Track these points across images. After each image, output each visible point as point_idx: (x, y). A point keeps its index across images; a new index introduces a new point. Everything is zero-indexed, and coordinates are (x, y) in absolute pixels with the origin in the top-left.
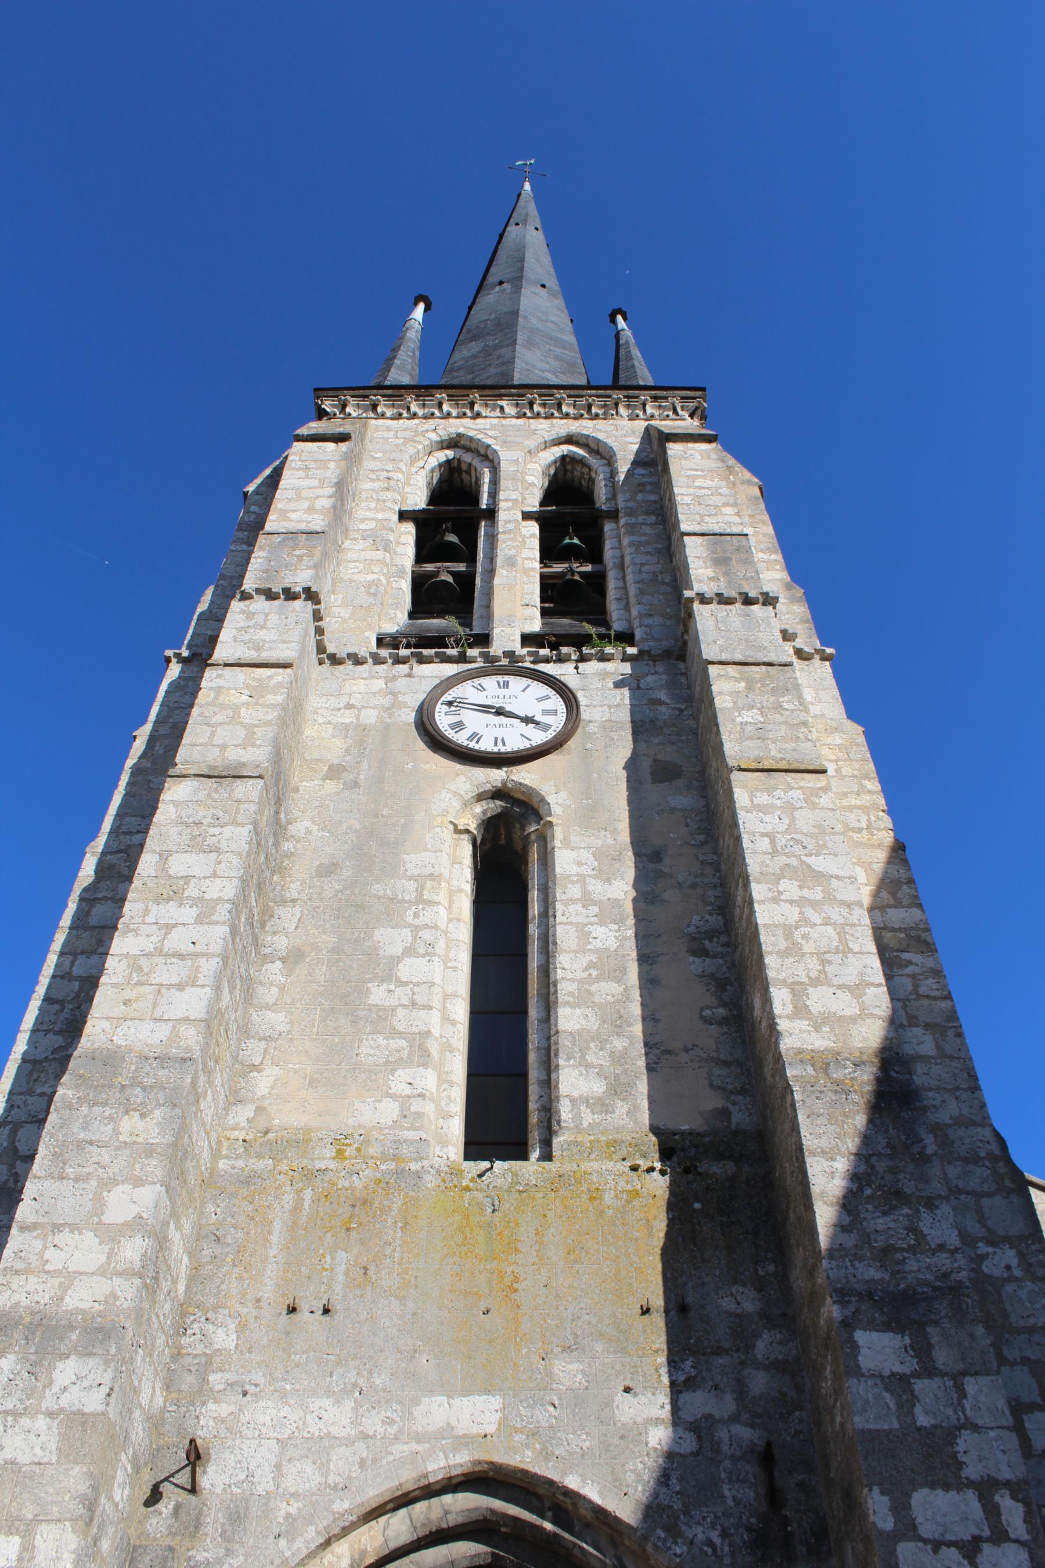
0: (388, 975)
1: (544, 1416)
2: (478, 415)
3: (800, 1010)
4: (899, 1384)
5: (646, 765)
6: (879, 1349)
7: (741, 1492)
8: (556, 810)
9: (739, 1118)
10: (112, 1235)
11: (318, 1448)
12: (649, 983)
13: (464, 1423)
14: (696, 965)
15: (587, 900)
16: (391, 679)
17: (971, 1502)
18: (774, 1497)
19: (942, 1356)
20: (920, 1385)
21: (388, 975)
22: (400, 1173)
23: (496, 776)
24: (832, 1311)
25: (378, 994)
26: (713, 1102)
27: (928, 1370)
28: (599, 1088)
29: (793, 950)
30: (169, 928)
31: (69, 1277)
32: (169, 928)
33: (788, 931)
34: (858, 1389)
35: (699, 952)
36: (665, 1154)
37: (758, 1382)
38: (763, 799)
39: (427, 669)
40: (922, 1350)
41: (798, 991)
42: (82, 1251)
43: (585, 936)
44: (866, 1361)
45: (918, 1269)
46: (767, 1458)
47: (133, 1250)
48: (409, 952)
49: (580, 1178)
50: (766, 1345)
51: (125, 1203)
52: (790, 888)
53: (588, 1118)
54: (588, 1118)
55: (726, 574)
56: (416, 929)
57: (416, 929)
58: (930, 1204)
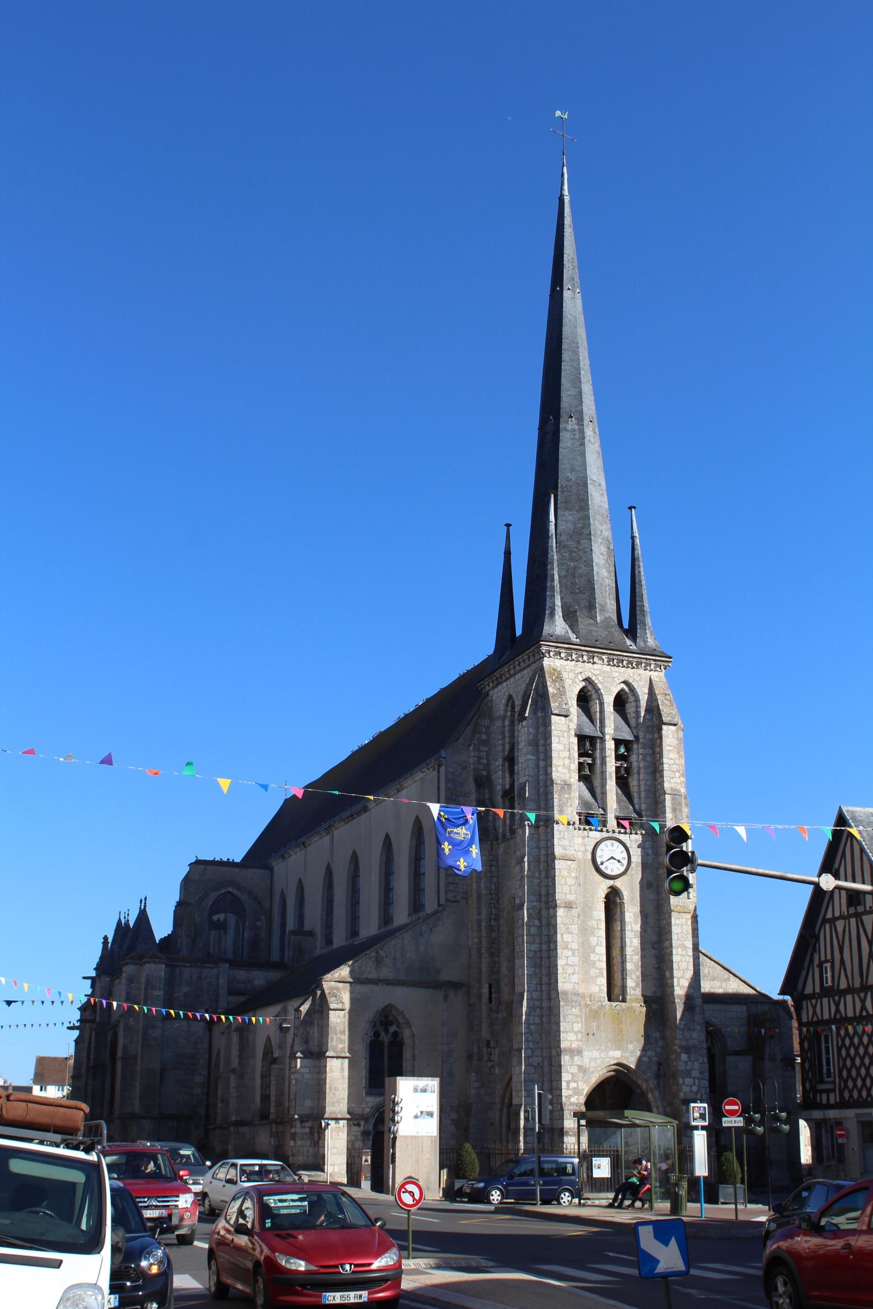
0: (594, 952)
1: (627, 1055)
2: (594, 663)
3: (679, 984)
4: (686, 1063)
5: (645, 881)
6: (684, 1057)
7: (654, 1068)
8: (625, 898)
9: (658, 994)
10: (576, 1033)
11: (595, 1059)
12: (643, 957)
13: (615, 1055)
14: (653, 952)
15: (632, 931)
16: (584, 838)
17: (692, 1080)
18: (659, 1069)
19: (692, 1058)
20: (689, 1063)
21: (594, 952)
22: (602, 1005)
23: (611, 883)
24: (677, 1048)
25: (593, 957)
26: (654, 989)
27: (690, 1060)
28: (634, 984)
29: (679, 969)
30: (567, 957)
31: (572, 1041)
32: (567, 957)
33: (678, 963)
34: (680, 1063)
35: (654, 948)
36: (645, 1002)
37: (658, 1050)
38: (677, 922)
39: (592, 834)
40: (689, 1057)
41: (678, 981)
42: (571, 1037)
43: (632, 942)
44: (682, 1059)
45: (691, 1042)
46: (659, 1064)
47: (580, 1036)
48: (597, 944)
49: (632, 1007)
50: (660, 1043)
51: (577, 1027)
52: (680, 950)
53: (632, 992)
54: (632, 992)
55: (675, 817)
56: (598, 937)
57: (598, 937)
58: (694, 1030)
